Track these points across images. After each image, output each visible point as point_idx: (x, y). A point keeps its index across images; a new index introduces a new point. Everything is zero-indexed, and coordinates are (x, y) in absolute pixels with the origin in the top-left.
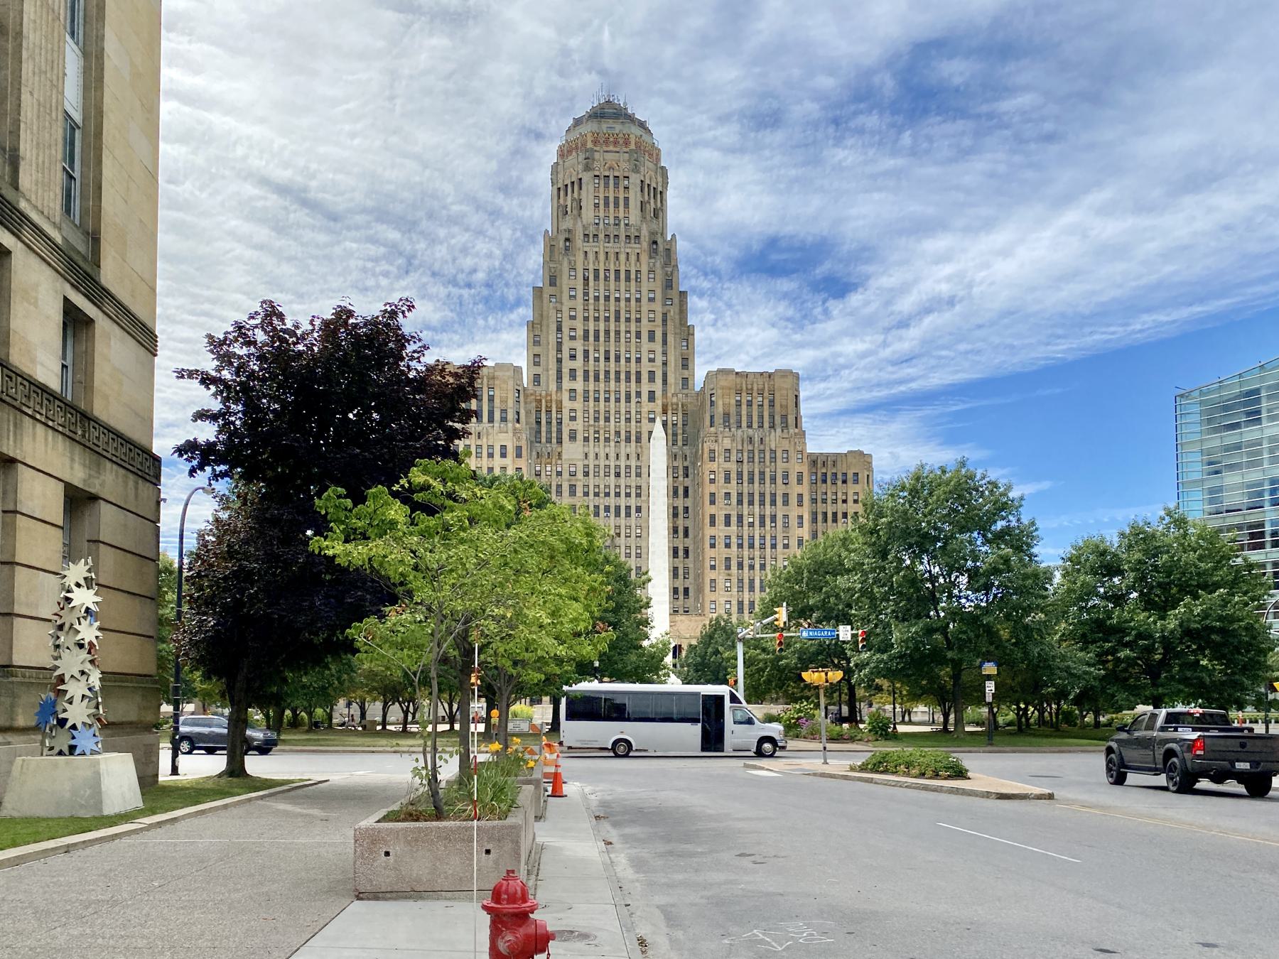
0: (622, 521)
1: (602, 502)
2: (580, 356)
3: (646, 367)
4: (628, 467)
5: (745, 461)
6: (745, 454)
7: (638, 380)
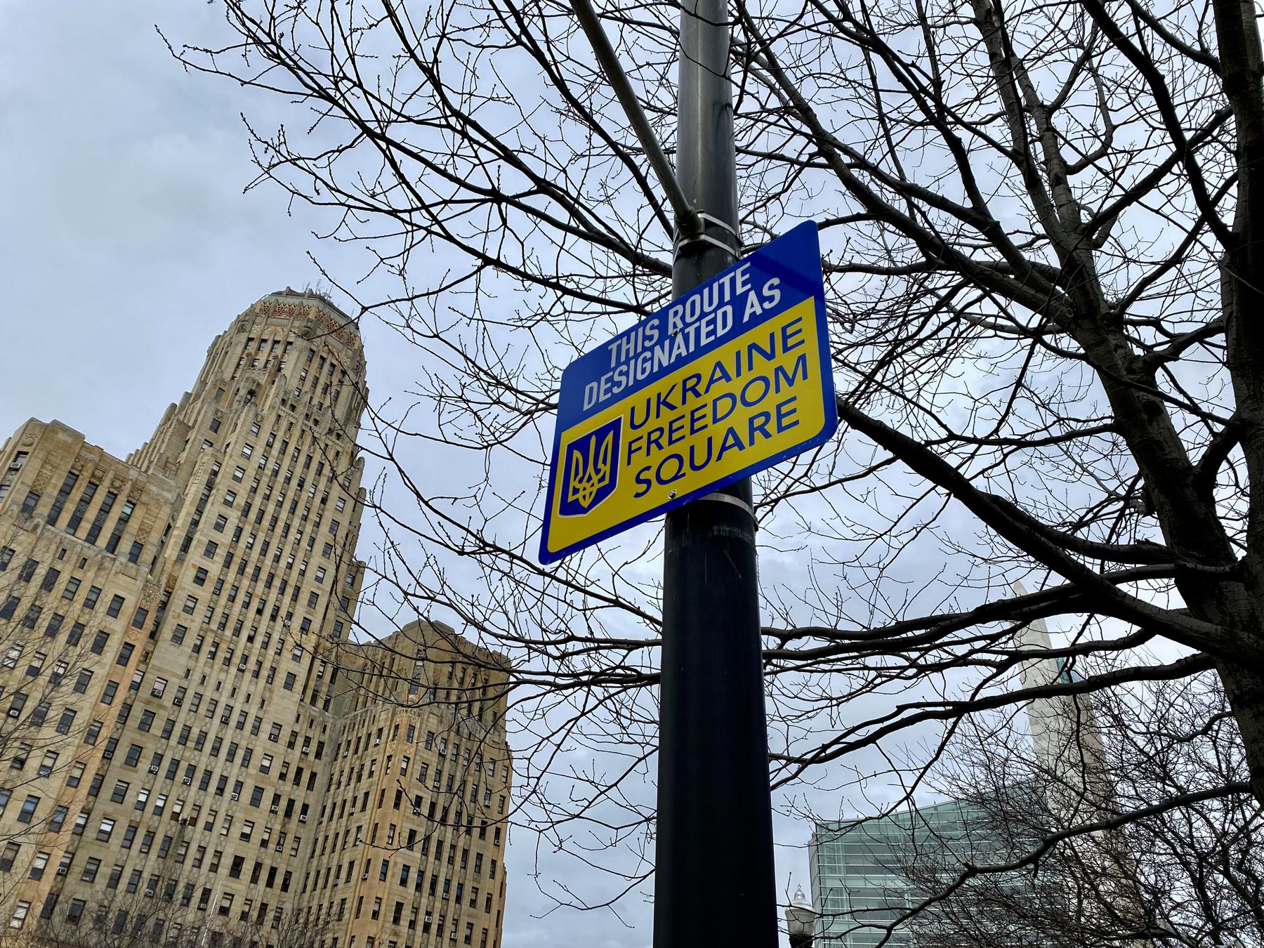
0: (208, 800)
1: (189, 756)
2: (230, 529)
3: (309, 586)
4: (245, 714)
5: (449, 756)
6: (450, 746)
7: (295, 598)
